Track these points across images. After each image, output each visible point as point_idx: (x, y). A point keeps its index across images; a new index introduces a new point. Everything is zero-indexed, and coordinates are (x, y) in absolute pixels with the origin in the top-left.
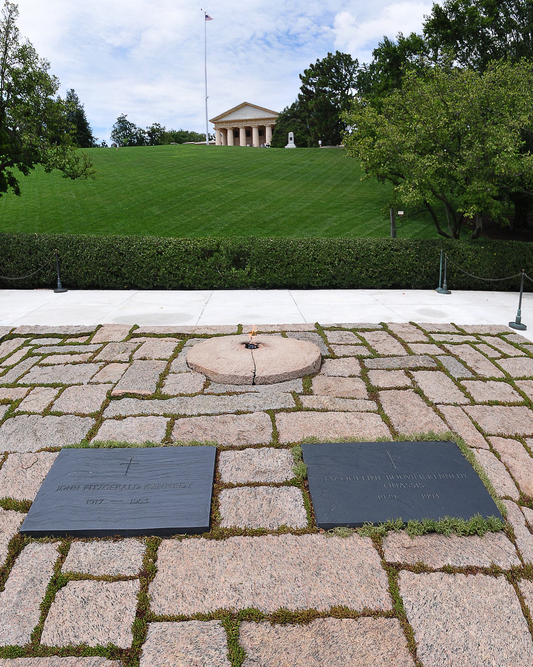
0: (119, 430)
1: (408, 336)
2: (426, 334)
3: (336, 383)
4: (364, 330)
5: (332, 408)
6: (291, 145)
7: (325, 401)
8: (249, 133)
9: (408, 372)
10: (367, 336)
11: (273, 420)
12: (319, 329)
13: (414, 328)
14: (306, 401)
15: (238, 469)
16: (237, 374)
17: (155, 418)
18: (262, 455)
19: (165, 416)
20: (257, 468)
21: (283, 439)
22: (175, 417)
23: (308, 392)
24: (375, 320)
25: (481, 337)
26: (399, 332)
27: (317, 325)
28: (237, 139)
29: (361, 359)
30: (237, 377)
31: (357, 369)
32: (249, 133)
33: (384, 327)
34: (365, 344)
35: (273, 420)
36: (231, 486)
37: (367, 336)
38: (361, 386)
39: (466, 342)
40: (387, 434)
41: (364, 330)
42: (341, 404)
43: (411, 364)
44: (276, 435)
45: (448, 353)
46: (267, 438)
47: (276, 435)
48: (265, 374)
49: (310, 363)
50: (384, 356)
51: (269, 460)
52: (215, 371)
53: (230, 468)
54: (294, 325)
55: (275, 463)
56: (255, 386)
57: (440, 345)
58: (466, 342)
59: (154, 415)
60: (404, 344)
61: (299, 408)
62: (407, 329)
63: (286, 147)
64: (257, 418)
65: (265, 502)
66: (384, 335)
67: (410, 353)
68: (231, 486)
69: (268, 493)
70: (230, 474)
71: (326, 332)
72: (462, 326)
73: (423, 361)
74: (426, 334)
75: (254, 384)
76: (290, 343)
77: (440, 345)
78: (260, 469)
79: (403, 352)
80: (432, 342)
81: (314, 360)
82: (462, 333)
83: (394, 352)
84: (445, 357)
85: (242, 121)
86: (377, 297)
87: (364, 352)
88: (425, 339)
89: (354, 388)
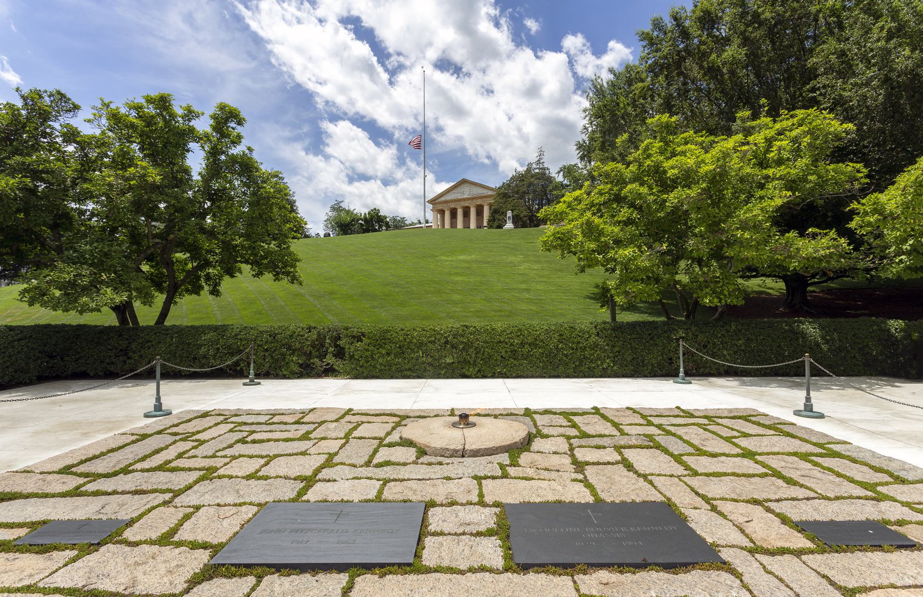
0: (331, 490)
1: (622, 419)
2: (643, 417)
3: (543, 458)
4: (575, 414)
5: (537, 477)
7: (530, 472)
8: (466, 214)
9: (618, 448)
10: (577, 419)
11: (480, 485)
12: (528, 413)
14: (512, 471)
15: (444, 521)
16: (448, 447)
17: (368, 481)
18: (467, 510)
19: (378, 480)
21: (488, 499)
23: (514, 464)
24: (587, 405)
26: (613, 416)
27: (527, 410)
28: (453, 220)
29: (568, 438)
30: (448, 450)
31: (565, 447)
32: (466, 214)
33: (596, 411)
34: (574, 426)
35: (480, 485)
37: (577, 419)
38: (567, 460)
39: (693, 424)
40: (591, 499)
41: (575, 414)
42: (545, 474)
43: (622, 443)
44: (481, 495)
45: (668, 433)
47: (481, 495)
48: (474, 447)
49: (517, 440)
50: (593, 437)
52: (428, 444)
53: (437, 520)
54: (505, 409)
55: (479, 518)
56: (464, 459)
57: (659, 427)
58: (693, 424)
59: (368, 478)
60: (616, 425)
61: (505, 476)
62: (622, 413)
64: (465, 483)
65: (467, 548)
67: (622, 433)
69: (470, 541)
71: (535, 416)
73: (637, 440)
74: (643, 417)
75: (463, 456)
76: (501, 423)
77: (659, 427)
80: (650, 424)
81: (521, 437)
82: (689, 414)
83: (607, 432)
84: (664, 437)
85: (460, 200)
89: (560, 463)
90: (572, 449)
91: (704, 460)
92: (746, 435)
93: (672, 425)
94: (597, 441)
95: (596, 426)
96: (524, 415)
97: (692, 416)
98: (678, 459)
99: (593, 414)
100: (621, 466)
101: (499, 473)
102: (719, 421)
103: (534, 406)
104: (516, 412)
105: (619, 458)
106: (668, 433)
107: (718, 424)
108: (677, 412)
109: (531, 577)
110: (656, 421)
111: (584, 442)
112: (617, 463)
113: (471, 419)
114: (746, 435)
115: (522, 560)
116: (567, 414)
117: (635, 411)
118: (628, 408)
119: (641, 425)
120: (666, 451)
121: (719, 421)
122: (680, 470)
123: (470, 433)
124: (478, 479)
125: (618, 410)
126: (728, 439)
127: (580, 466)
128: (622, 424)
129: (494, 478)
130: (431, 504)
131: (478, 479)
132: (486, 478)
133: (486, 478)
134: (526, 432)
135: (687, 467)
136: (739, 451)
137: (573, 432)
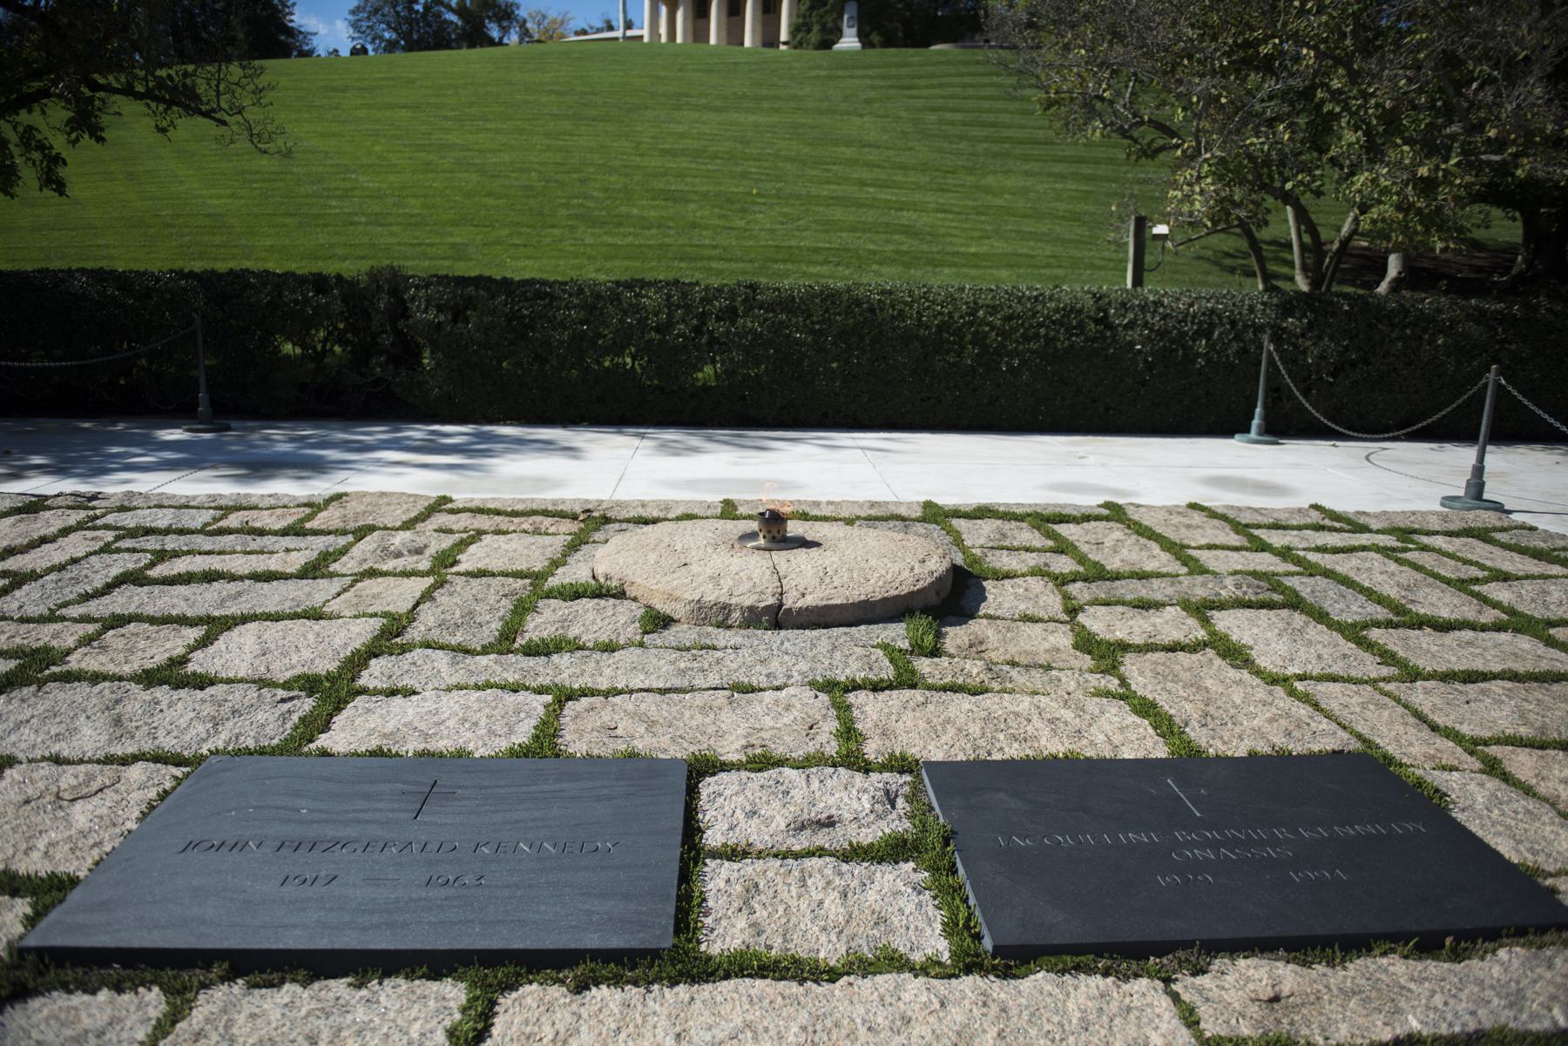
2: (1239, 528)
6: (849, 41)
13: (1197, 518)
14: (924, 665)
20: (806, 811)
22: (565, 696)
25: (1415, 537)
29: (1061, 581)
34: (1063, 547)
36: (734, 854)
37: (1064, 530)
46: (827, 740)
51: (837, 796)
57: (1285, 553)
60: (1177, 550)
61: (907, 680)
63: (837, 47)
66: (1115, 533)
67: (1196, 568)
68: (734, 854)
70: (726, 826)
72: (1345, 512)
74: (1239, 528)
77: (1285, 553)
78: (813, 815)
79: (1176, 567)
80: (1263, 547)
86: (1081, 450)
87: (1064, 564)
88: (1235, 539)
90: (1073, 612)
91: (1425, 638)
92: (1505, 577)
93: (1318, 549)
94: (1131, 590)
95: (1115, 548)
96: (923, 520)
97: (1364, 529)
98: (1355, 633)
99: (1107, 519)
100: (1210, 652)
101: (887, 672)
102: (1425, 540)
103: (946, 500)
104: (903, 512)
105: (1201, 634)
106: (1311, 570)
107: (1424, 548)
108: (1315, 517)
109: (1039, 983)
110: (1276, 539)
111: (1100, 590)
112: (1203, 645)
113: (794, 528)
114: (1505, 577)
115: (1015, 937)
116: (1044, 520)
117: (1212, 514)
118: (1194, 506)
119: (1236, 549)
120: (1321, 617)
121: (1425, 540)
122: (1370, 666)
123: (798, 566)
124: (836, 690)
125: (1170, 511)
126: (1462, 585)
127: (1107, 655)
128: (1189, 547)
129: (876, 687)
130: (702, 768)
131: (836, 690)
132: (854, 686)
133: (854, 686)
134: (945, 565)
135: (1387, 657)
136: (1489, 616)
137: (1064, 564)
